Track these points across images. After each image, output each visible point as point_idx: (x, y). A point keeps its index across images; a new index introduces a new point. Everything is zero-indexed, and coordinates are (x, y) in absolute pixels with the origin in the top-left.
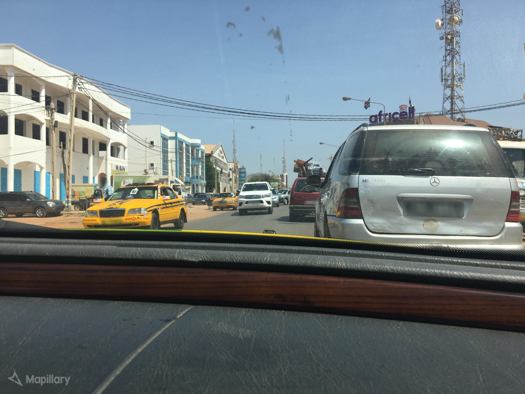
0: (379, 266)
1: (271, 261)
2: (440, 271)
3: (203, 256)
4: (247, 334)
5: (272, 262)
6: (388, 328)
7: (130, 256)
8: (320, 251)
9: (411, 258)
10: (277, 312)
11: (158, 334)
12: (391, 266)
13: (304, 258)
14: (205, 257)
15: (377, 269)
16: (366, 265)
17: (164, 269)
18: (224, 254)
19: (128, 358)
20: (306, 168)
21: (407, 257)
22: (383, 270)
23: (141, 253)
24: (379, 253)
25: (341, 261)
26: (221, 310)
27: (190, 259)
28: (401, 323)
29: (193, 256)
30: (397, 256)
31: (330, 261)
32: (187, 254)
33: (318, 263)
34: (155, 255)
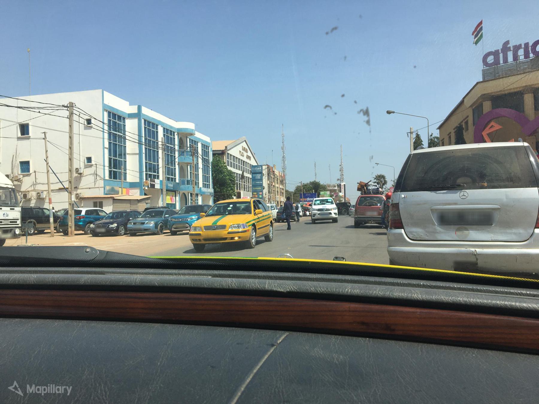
0: (453, 298)
1: (352, 292)
2: (510, 303)
3: (290, 287)
4: (341, 359)
5: (353, 293)
6: (464, 356)
7: (227, 287)
8: (395, 283)
9: (481, 289)
10: (362, 340)
11: (266, 357)
12: (464, 297)
13: (383, 290)
14: (292, 288)
15: (451, 300)
16: (441, 296)
17: (256, 298)
18: (309, 286)
19: (248, 378)
20: (367, 188)
21: (479, 288)
22: (457, 302)
23: (236, 284)
24: (451, 285)
25: (416, 292)
26: (312, 336)
27: (279, 290)
28: (476, 351)
29: (281, 287)
30: (468, 287)
31: (406, 293)
32: (276, 285)
33: (395, 295)
34: (248, 285)
